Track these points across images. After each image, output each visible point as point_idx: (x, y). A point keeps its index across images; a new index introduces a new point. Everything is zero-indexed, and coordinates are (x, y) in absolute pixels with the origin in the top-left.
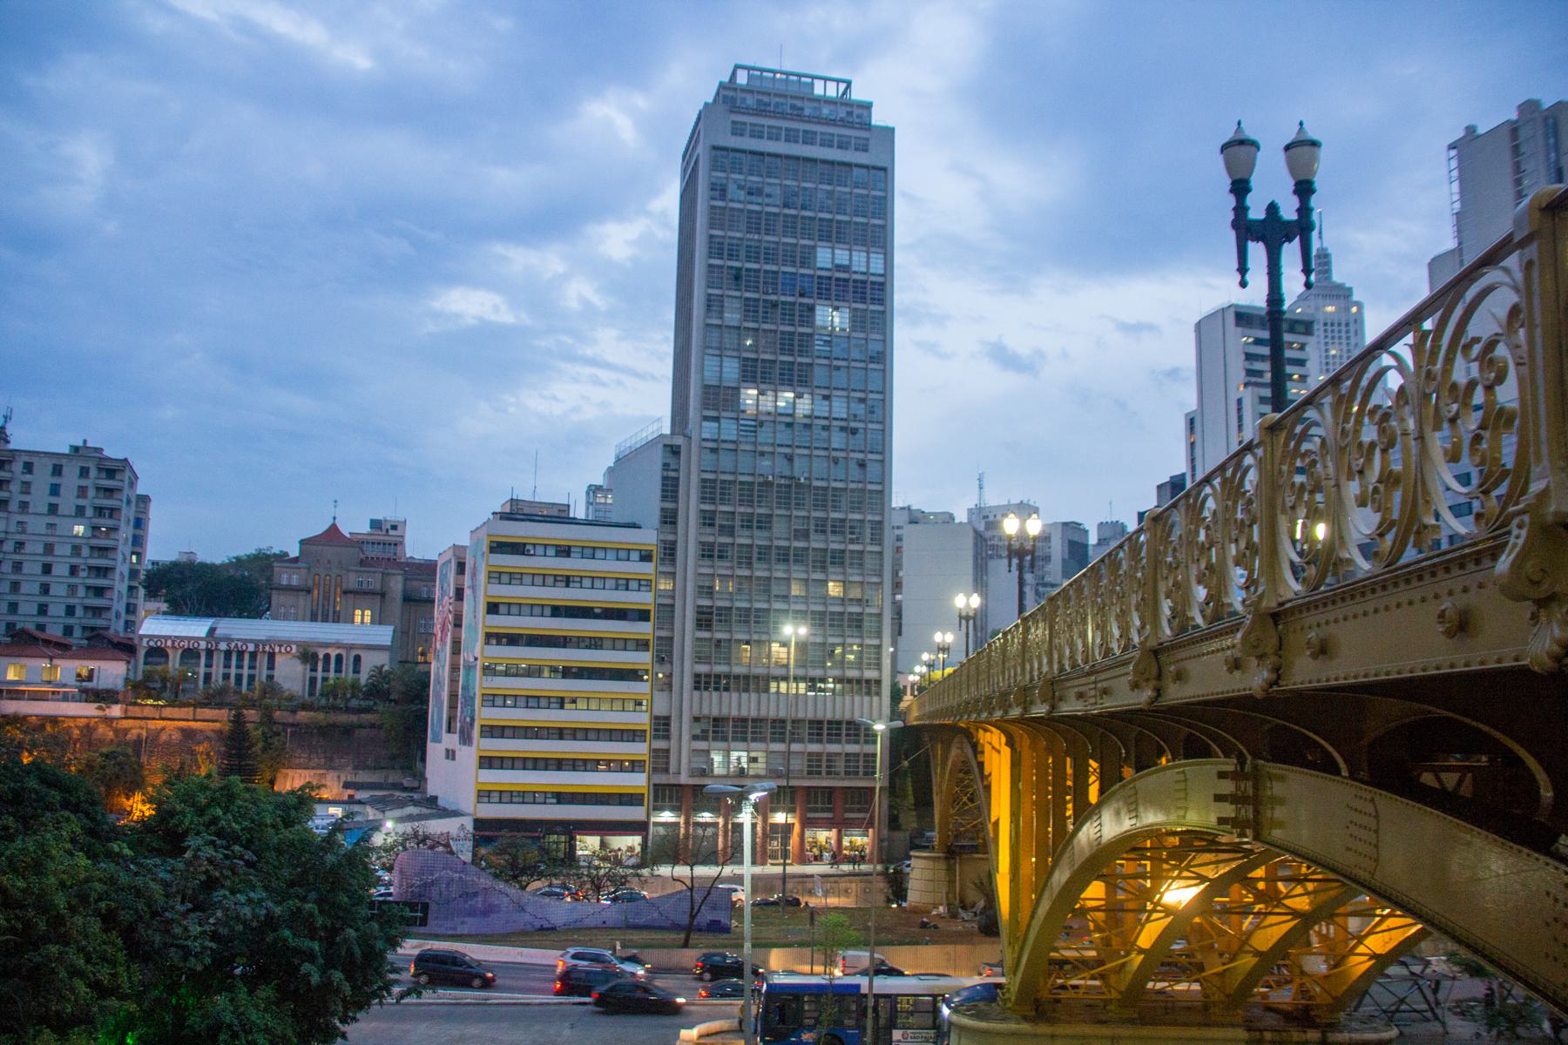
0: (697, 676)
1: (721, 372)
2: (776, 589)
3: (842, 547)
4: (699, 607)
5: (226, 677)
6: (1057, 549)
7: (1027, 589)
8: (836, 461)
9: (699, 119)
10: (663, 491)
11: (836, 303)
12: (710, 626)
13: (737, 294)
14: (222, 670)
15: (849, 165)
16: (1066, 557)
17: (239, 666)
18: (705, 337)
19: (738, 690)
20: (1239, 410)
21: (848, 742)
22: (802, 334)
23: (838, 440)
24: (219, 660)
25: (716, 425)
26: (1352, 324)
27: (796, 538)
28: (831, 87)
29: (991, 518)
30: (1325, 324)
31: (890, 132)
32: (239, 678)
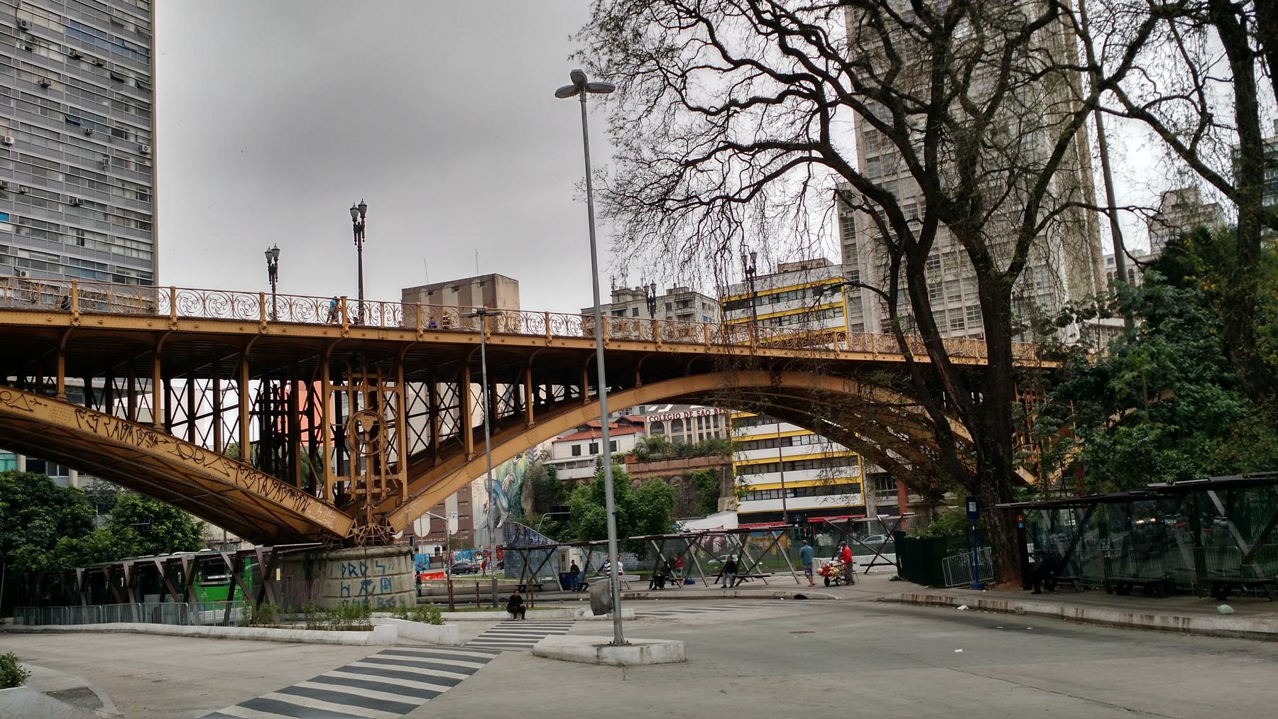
5: (701, 436)
14: (697, 432)
17: (708, 427)
24: (694, 424)
32: (709, 434)
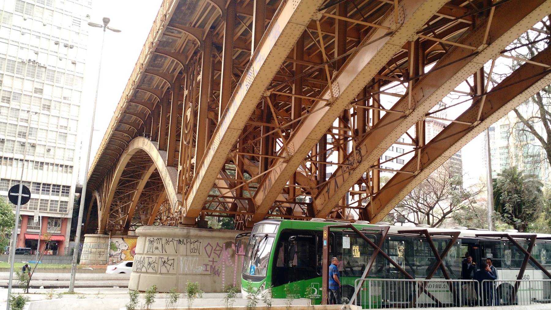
3: (60, 100)
21: (52, 195)
23: (62, 49)
27: (36, 92)
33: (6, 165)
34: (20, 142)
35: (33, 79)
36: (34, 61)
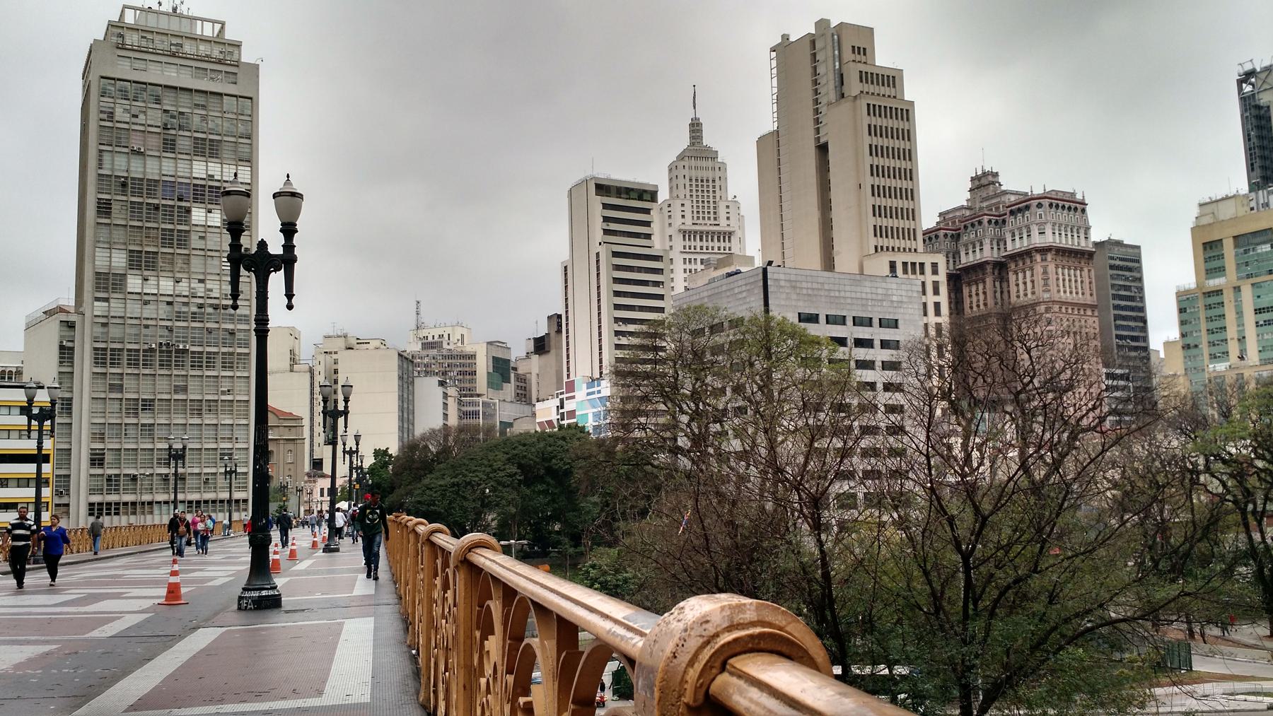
0: (91, 504)
1: (110, 261)
2: (158, 433)
3: (216, 398)
4: (91, 449)
6: (482, 366)
7: (450, 401)
8: (210, 331)
9: (90, 52)
10: (60, 358)
11: (210, 206)
12: (102, 464)
13: (124, 198)
15: (220, 94)
16: (491, 371)
18: (95, 233)
19: (127, 514)
20: (598, 261)
22: (179, 231)
25: (107, 304)
26: (717, 179)
27: (176, 392)
28: (208, 26)
29: (430, 339)
30: (697, 180)
31: (256, 67)
33: (143, 513)
34: (161, 475)
35: (169, 373)
36: (169, 344)
